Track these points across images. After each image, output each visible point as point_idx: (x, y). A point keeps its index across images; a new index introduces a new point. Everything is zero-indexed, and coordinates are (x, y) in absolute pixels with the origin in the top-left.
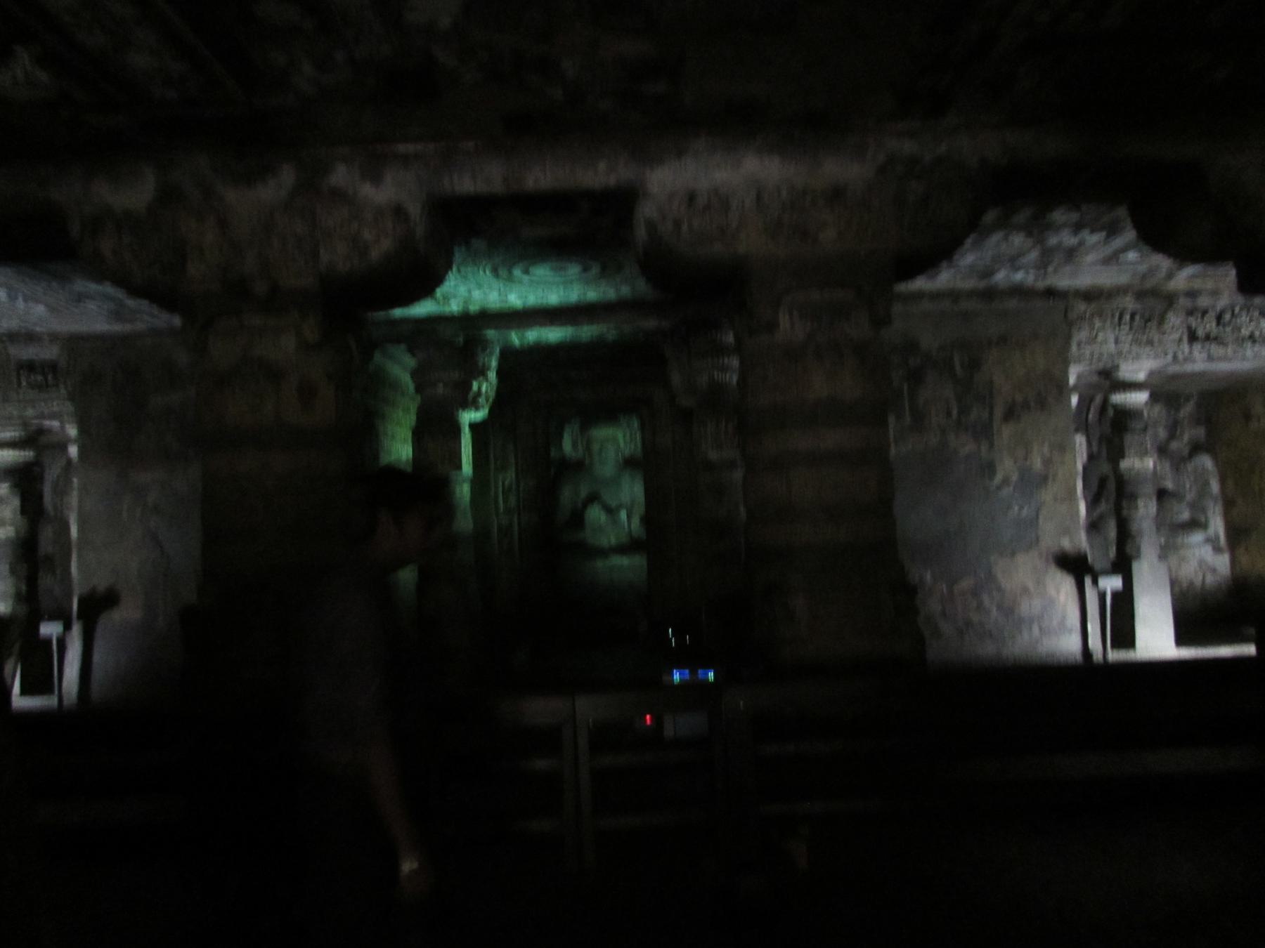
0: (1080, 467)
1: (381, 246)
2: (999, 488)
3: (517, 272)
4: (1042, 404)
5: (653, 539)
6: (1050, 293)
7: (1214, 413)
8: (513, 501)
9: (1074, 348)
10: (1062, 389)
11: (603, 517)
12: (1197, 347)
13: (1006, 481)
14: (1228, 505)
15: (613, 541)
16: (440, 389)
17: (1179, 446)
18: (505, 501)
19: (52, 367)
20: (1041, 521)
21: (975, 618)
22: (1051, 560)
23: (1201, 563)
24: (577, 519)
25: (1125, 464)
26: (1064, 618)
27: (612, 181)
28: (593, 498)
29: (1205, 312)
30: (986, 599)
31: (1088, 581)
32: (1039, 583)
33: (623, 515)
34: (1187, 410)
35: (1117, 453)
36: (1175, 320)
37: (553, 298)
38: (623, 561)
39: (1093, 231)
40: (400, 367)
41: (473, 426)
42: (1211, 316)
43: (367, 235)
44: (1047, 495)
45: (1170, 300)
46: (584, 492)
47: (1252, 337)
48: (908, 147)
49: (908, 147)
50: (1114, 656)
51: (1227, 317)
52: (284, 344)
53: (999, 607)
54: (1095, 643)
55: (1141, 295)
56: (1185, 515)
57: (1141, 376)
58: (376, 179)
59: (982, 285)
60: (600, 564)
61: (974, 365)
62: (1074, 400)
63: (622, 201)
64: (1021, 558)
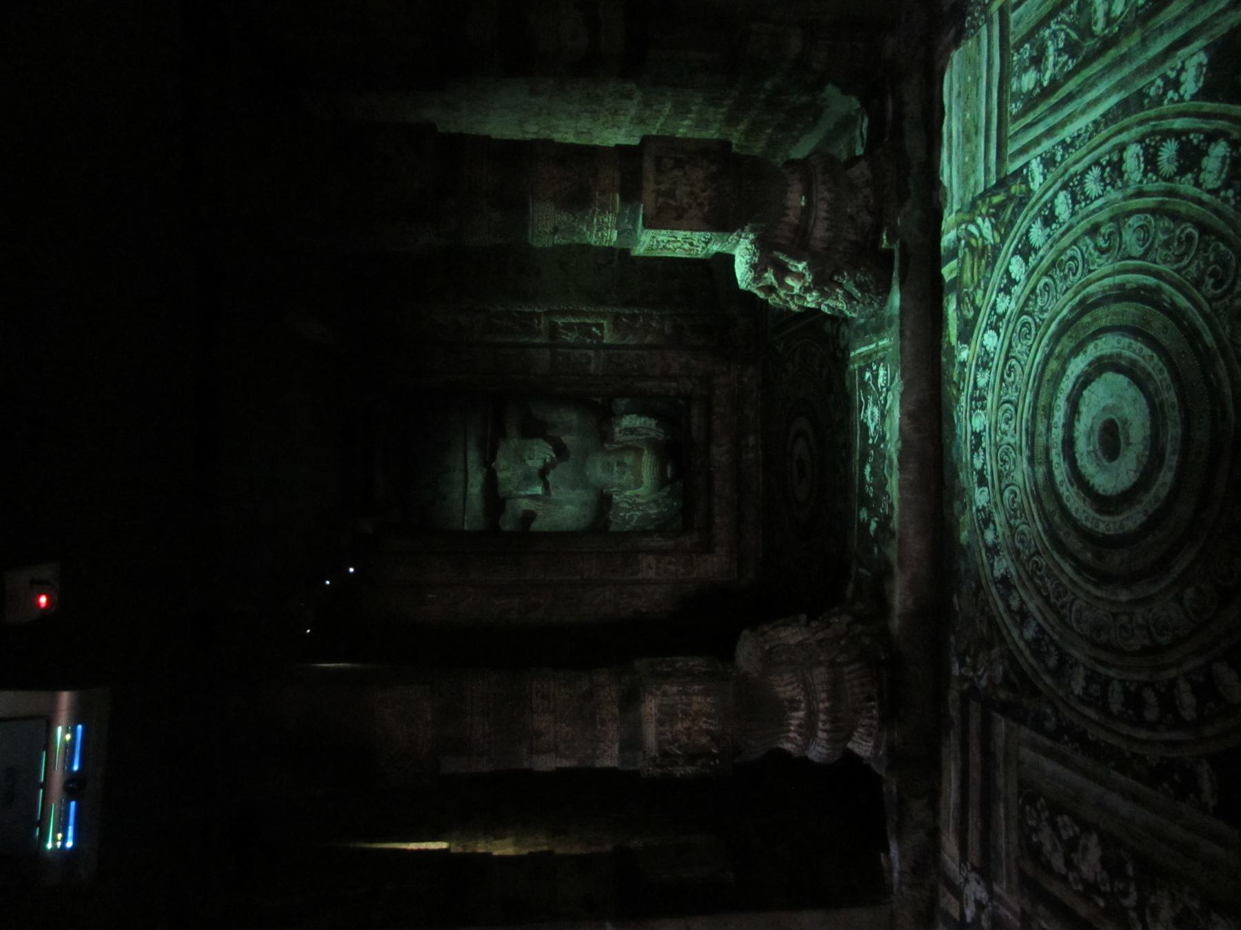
8: (571, 338)
11: (536, 464)
15: (501, 475)
18: (569, 327)
24: (534, 429)
28: (561, 451)
33: (539, 490)
38: (475, 489)
41: (729, 260)
46: (567, 439)
60: (473, 456)
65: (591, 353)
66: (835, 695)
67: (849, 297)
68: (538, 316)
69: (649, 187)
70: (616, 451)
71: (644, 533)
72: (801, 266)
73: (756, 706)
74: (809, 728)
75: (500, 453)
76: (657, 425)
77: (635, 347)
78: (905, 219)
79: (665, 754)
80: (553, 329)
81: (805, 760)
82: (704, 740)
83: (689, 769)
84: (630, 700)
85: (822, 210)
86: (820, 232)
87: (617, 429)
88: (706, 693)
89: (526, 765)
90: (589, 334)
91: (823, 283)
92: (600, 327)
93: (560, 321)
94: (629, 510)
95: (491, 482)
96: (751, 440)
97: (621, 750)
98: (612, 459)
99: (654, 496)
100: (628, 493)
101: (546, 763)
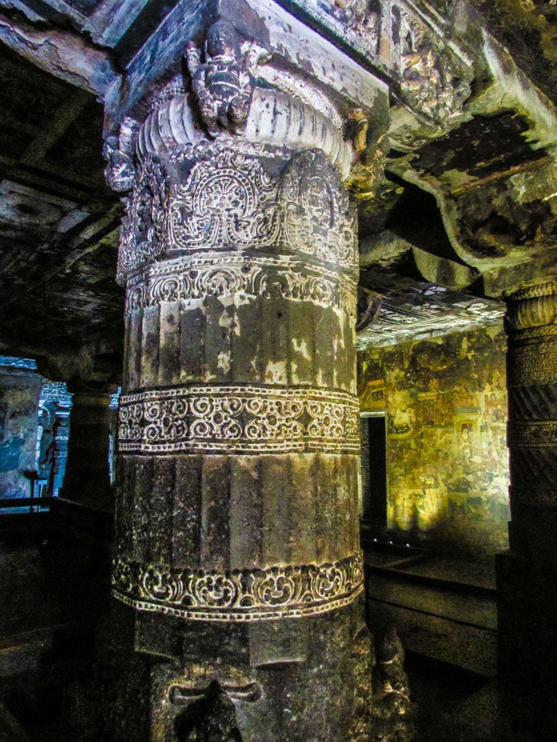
0: (39, 438)
2: (4, 444)
9: (42, 394)
10: (36, 408)
13: (7, 442)
25: (57, 438)
32: (16, 482)
44: (23, 449)
64: (9, 472)
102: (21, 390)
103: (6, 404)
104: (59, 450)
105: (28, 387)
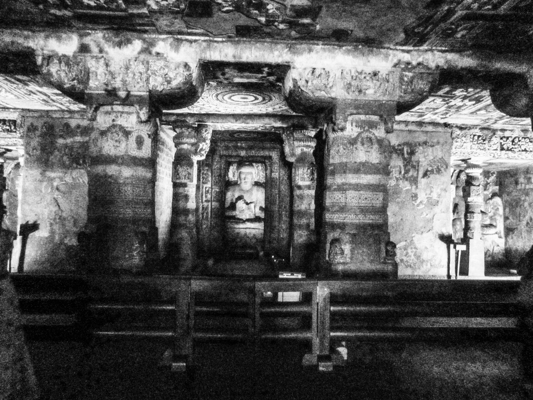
1: (177, 80)
2: (418, 205)
3: (226, 97)
4: (439, 171)
5: (268, 216)
6: (446, 125)
7: (505, 181)
8: (209, 196)
9: (453, 150)
11: (245, 206)
12: (504, 152)
13: (421, 202)
14: (506, 218)
15: (248, 217)
16: (185, 146)
17: (489, 193)
18: (206, 197)
19: (14, 122)
20: (434, 220)
21: (405, 259)
22: (437, 236)
23: (493, 242)
24: (233, 206)
25: (469, 199)
26: (440, 261)
27: (280, 61)
28: (240, 198)
29: (508, 138)
30: (409, 251)
31: (452, 246)
34: (492, 178)
35: (467, 194)
36: (496, 140)
37: (238, 110)
39: (470, 101)
40: (167, 135)
41: (199, 162)
42: (510, 139)
43: (171, 75)
44: (437, 209)
45: (494, 131)
46: (236, 196)
47: (525, 150)
48: (406, 57)
49: (406, 57)
50: (460, 278)
51: (516, 140)
52: (132, 119)
53: (415, 255)
54: (452, 273)
55: (483, 129)
56: (488, 222)
57: (480, 163)
58: (177, 49)
59: (418, 119)
60: (241, 226)
61: (412, 153)
62: (452, 170)
63: (280, 70)
64: (425, 235)
65: (213, 190)
66: (300, 140)
67: (208, 133)
68: (203, 205)
69: (183, 181)
70: (240, 179)
71: (266, 174)
72: (201, 146)
73: (302, 159)
74: (308, 147)
75: (241, 218)
76: (232, 166)
77: (212, 177)
78: (190, 121)
79: (312, 180)
80: (206, 201)
81: (315, 147)
82: (309, 171)
83: (315, 174)
84: (299, 187)
85: (188, 140)
86: (193, 141)
87: (233, 179)
88: (298, 170)
89: (313, 211)
90: (208, 191)
91: (204, 140)
92: (206, 188)
93: (204, 199)
94: (260, 176)
95: (249, 220)
96: (239, 144)
97: (310, 190)
98: (243, 181)
99: (255, 167)
100: (254, 176)
101: (313, 206)
102: (432, 146)
103: (418, 162)
104: (473, 213)
105: (438, 143)
